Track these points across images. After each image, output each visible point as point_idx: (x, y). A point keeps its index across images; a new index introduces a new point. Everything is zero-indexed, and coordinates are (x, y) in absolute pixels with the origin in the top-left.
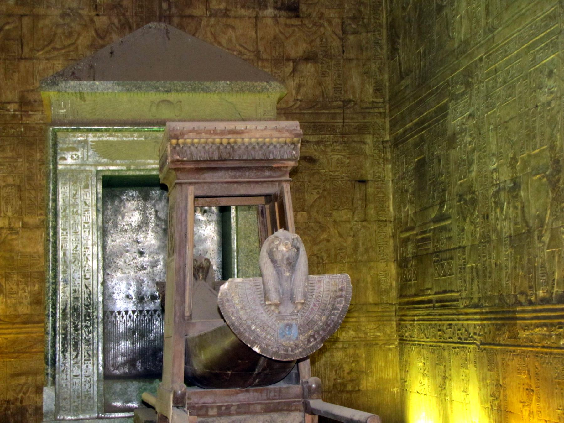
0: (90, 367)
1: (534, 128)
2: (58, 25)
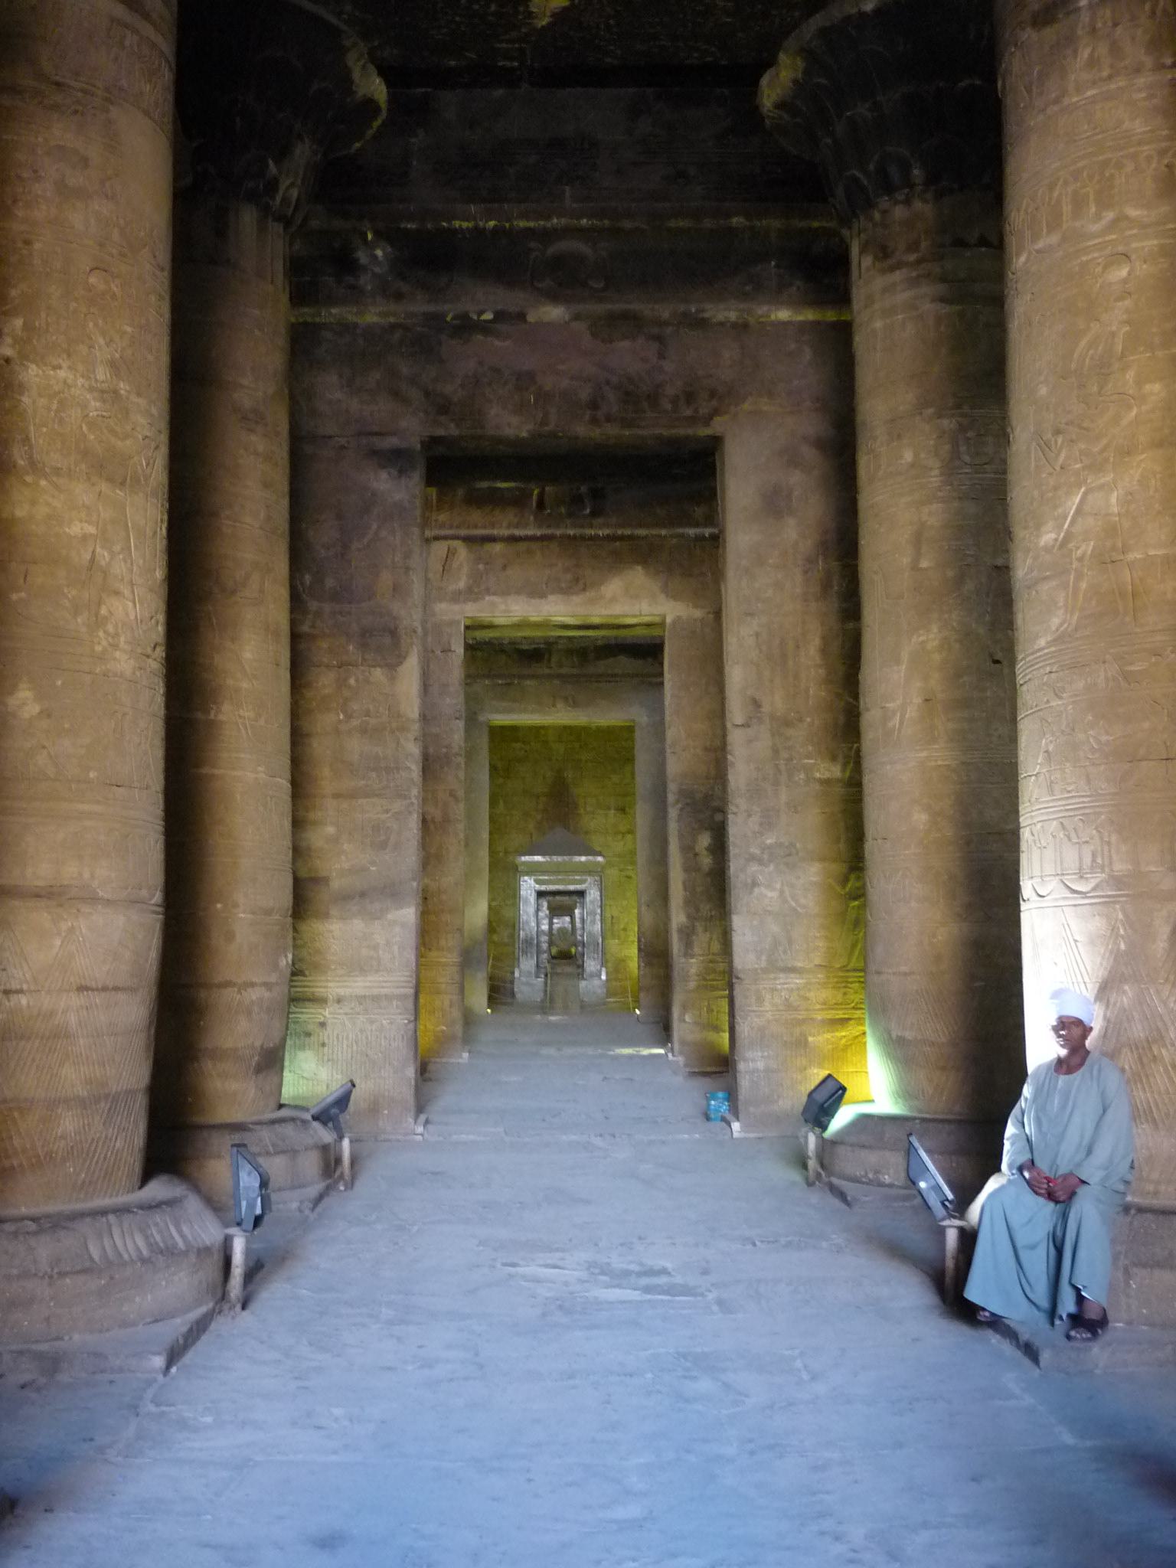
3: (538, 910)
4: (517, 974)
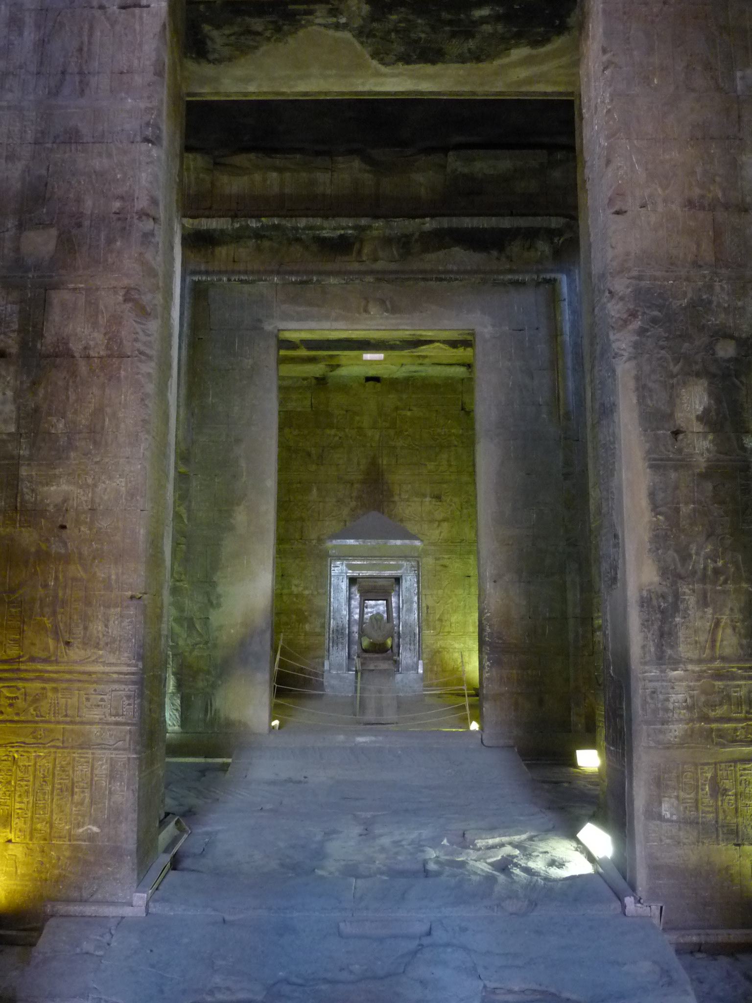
3: (350, 599)
4: (327, 667)
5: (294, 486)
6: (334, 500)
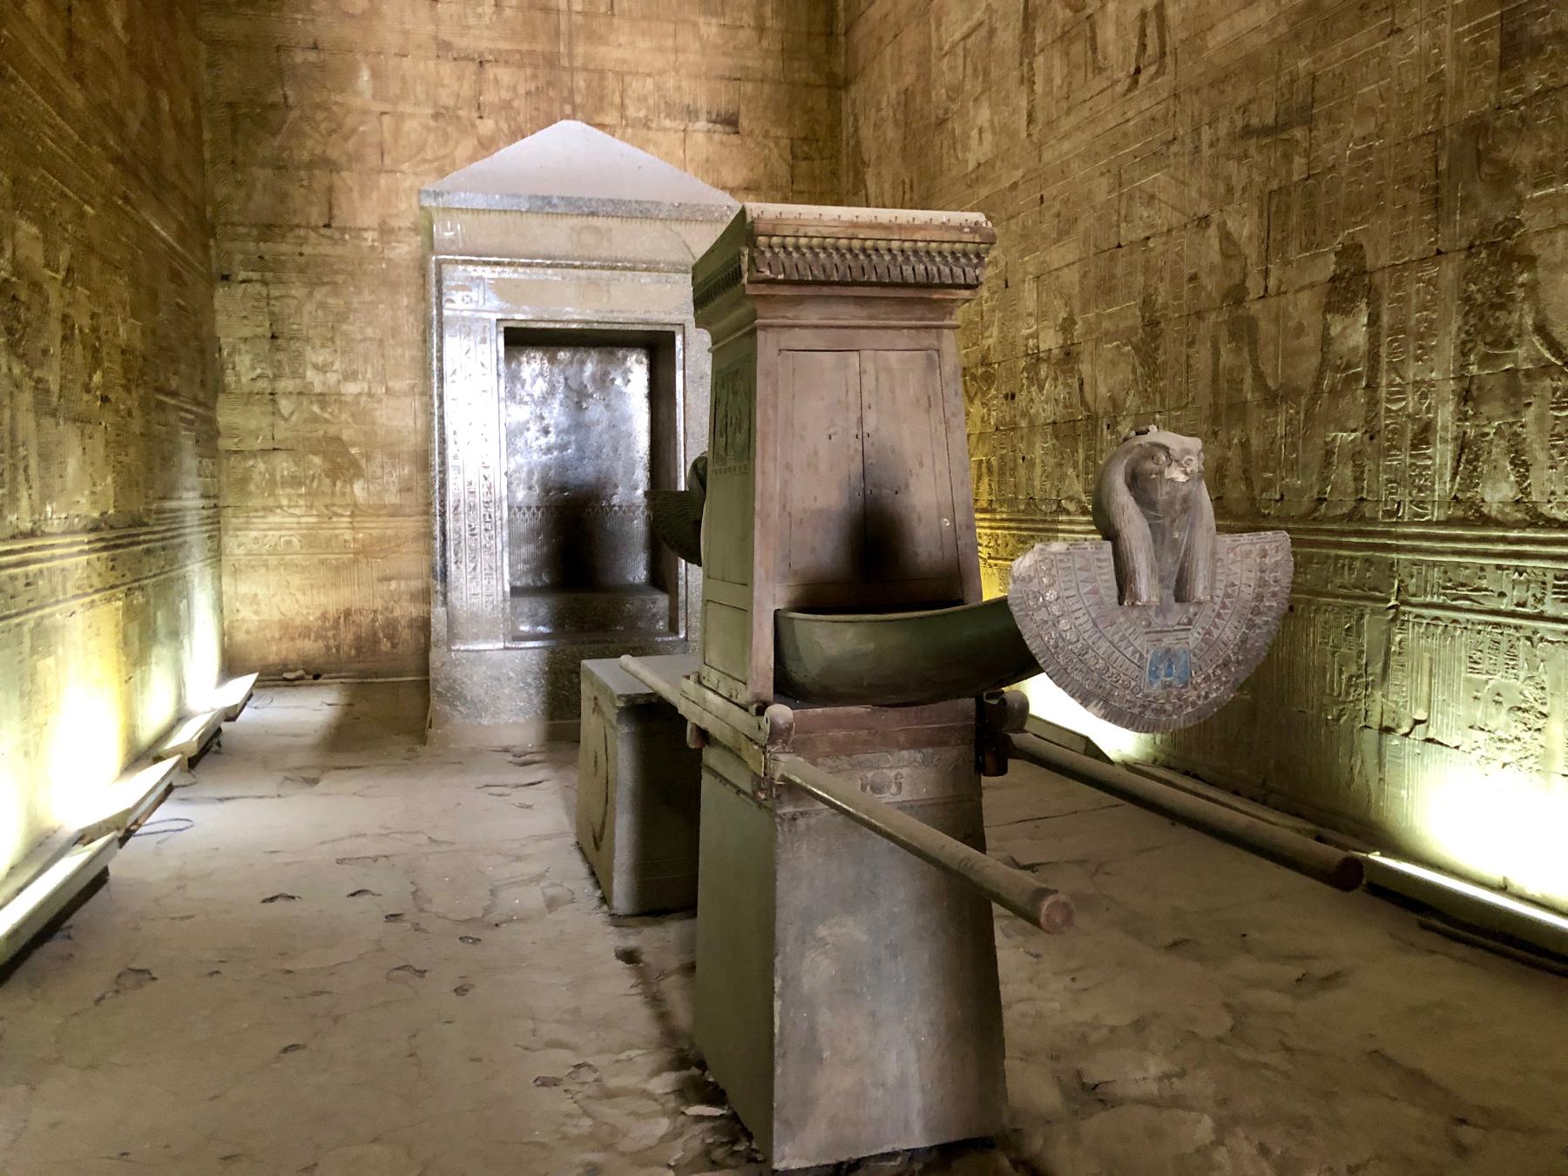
0: (493, 582)
1: (1113, 277)
2: (428, 128)
5: (299, 57)
6: (429, 111)
